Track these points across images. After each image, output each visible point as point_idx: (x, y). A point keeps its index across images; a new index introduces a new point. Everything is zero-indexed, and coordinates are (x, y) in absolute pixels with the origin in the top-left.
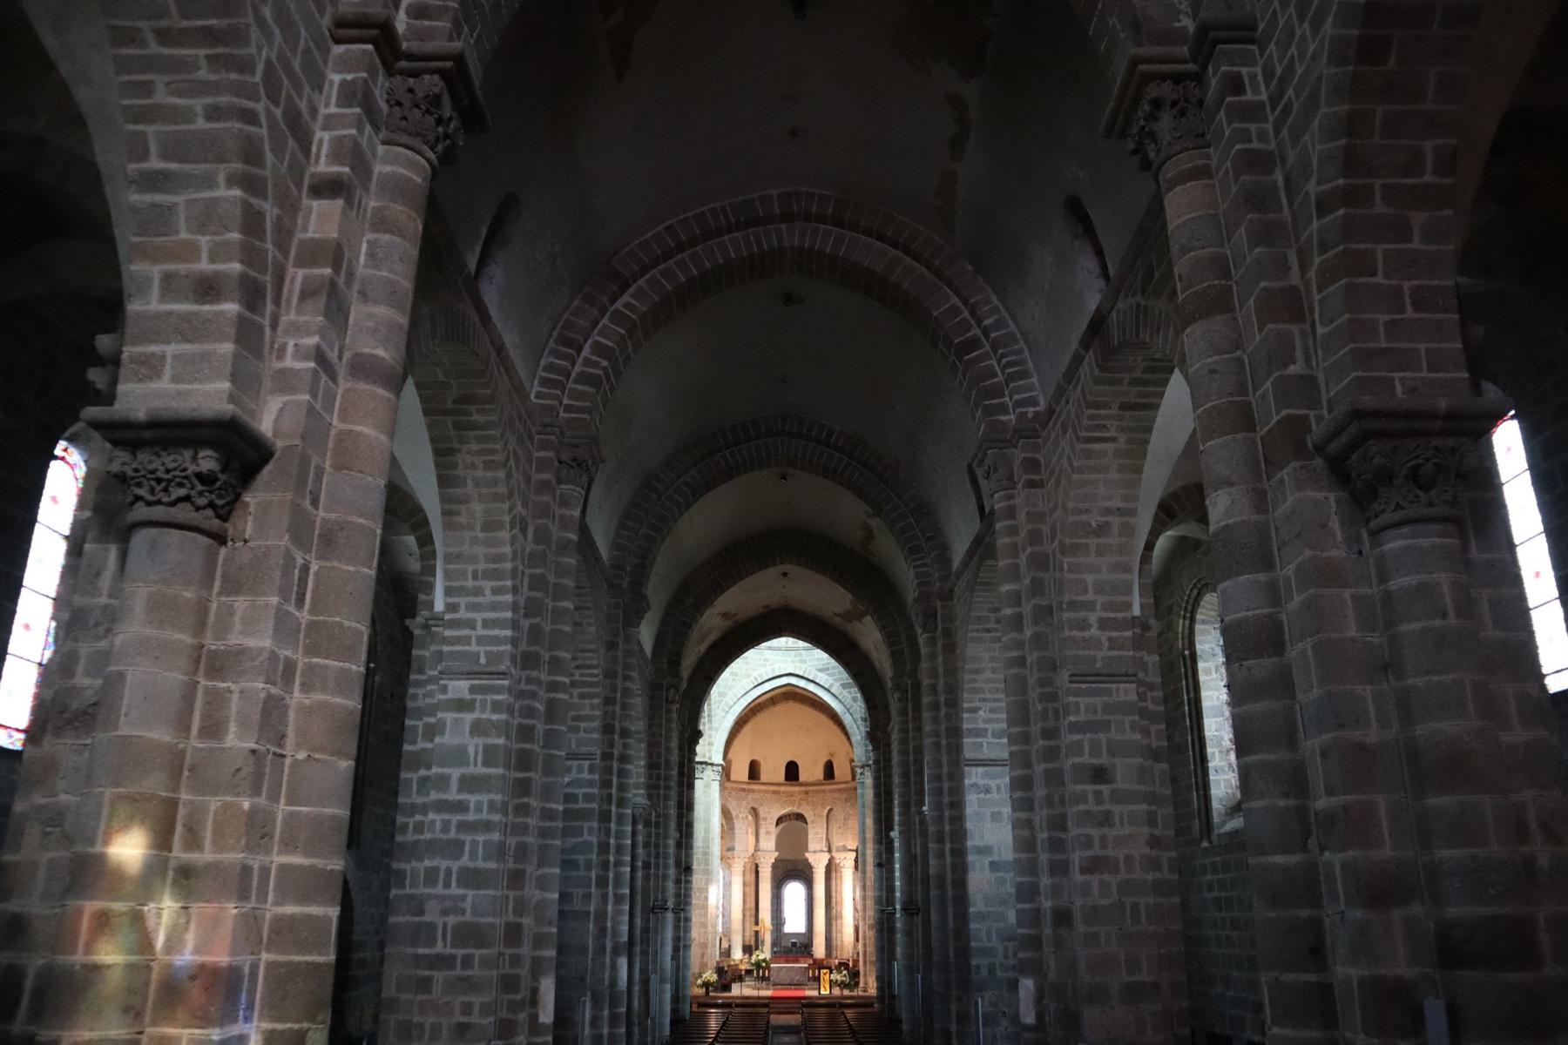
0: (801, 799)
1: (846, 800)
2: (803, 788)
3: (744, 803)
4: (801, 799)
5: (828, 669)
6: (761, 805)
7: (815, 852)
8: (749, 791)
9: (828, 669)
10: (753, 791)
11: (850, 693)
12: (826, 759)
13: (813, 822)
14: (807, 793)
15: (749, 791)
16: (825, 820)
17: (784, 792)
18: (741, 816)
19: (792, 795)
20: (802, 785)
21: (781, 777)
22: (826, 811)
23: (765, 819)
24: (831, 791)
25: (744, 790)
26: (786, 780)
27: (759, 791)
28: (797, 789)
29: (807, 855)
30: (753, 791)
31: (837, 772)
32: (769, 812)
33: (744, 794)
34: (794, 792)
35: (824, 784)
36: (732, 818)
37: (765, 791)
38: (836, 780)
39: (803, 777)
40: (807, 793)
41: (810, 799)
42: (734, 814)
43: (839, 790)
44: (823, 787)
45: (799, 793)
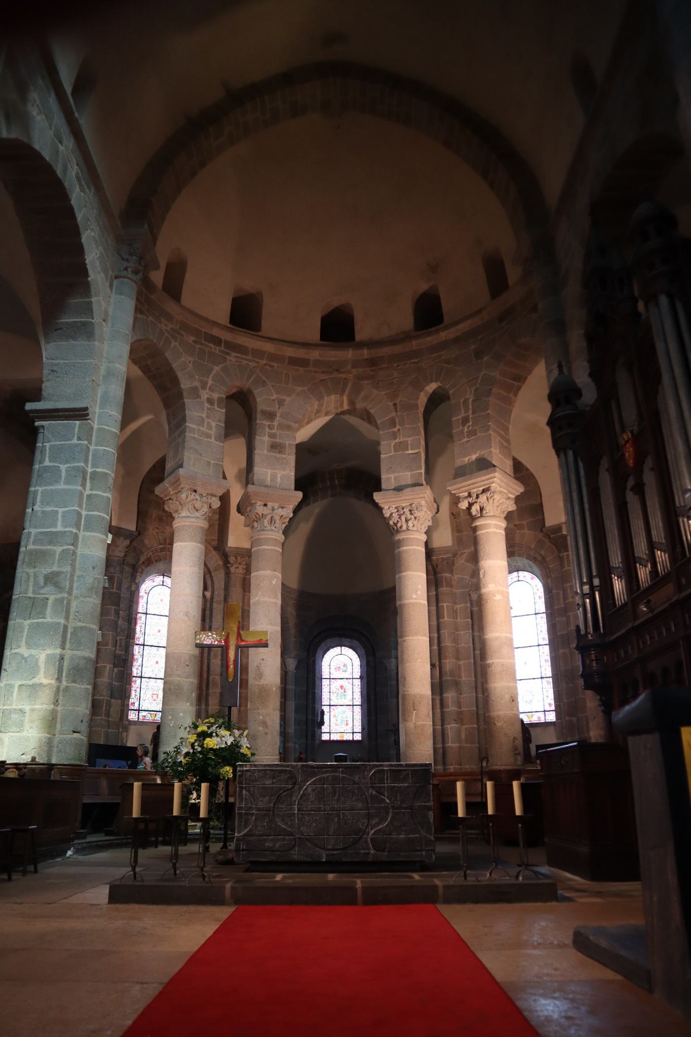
1: (478, 354)
2: (365, 353)
3: (216, 369)
6: (264, 384)
7: (399, 489)
8: (232, 347)
10: (241, 349)
12: (424, 286)
13: (393, 423)
15: (232, 347)
16: (421, 425)
17: (317, 363)
18: (205, 395)
21: (314, 333)
22: (423, 400)
23: (271, 416)
24: (444, 345)
25: (217, 341)
26: (322, 339)
27: (258, 354)
28: (349, 354)
29: (377, 497)
30: (241, 349)
31: (447, 305)
32: (281, 403)
36: (180, 395)
37: (273, 357)
38: (446, 321)
39: (362, 332)
40: (372, 362)
42: (185, 384)
43: (456, 340)
44: (414, 344)
45: (356, 364)
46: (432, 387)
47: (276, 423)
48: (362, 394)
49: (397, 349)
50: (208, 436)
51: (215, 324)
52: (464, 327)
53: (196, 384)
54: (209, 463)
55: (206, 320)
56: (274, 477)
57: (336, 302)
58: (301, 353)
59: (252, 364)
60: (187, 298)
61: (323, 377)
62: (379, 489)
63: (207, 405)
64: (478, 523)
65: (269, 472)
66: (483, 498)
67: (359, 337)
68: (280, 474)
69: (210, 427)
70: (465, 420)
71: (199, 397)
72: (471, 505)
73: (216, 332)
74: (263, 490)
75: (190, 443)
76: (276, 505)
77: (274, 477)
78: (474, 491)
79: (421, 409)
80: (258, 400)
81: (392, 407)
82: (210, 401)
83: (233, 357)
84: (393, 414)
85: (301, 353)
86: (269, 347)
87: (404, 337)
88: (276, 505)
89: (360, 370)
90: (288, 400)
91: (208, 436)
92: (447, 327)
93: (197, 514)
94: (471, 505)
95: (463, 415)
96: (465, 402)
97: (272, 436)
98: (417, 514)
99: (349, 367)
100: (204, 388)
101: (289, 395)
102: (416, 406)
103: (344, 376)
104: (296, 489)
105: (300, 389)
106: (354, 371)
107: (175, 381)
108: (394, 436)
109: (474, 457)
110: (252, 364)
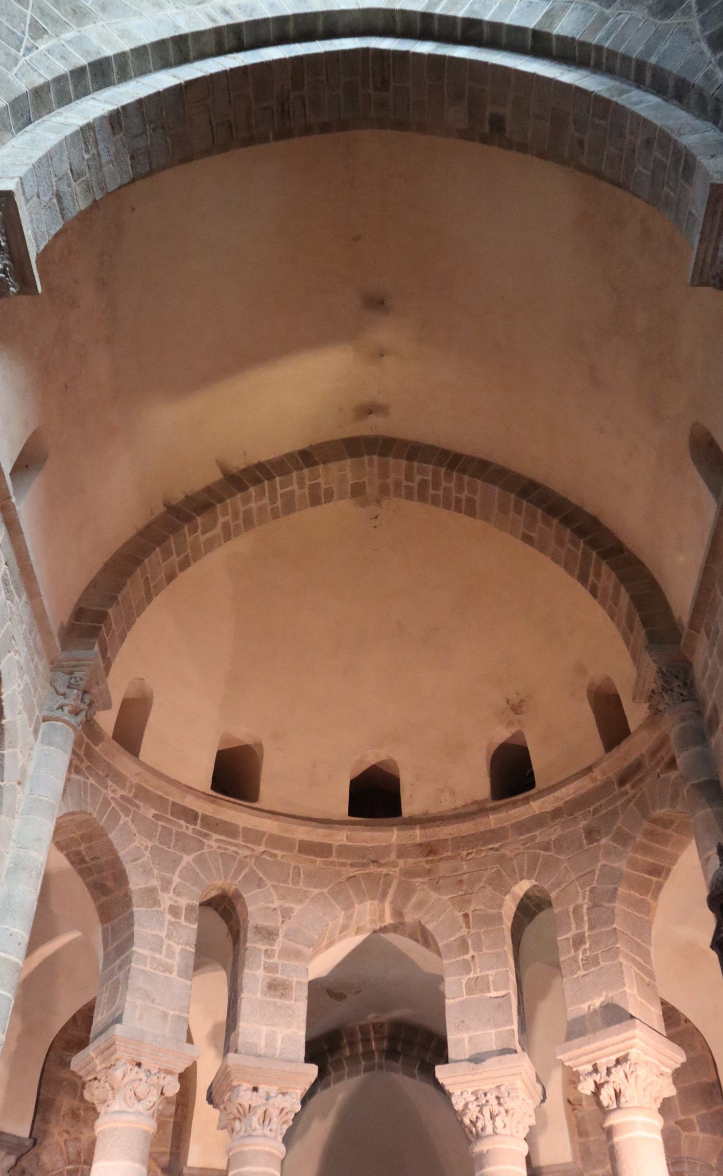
0: (410, 873)
1: (591, 834)
2: (418, 835)
3: (187, 859)
4: (410, 873)
6: (260, 884)
7: (477, 1059)
8: (212, 825)
10: (228, 830)
12: (502, 734)
13: (463, 946)
14: (429, 849)
15: (212, 825)
16: (508, 947)
17: (343, 850)
18: (166, 900)
19: (375, 857)
20: (413, 822)
21: (340, 806)
22: (509, 908)
23: (270, 935)
24: (539, 821)
25: (191, 816)
26: (351, 813)
30: (228, 830)
32: (286, 914)
33: (188, 829)
34: (385, 850)
35: (494, 810)
36: (126, 902)
37: (275, 841)
40: (429, 849)
41: (443, 868)
42: (136, 883)
43: (557, 813)
44: (492, 821)
45: (403, 852)
46: (523, 887)
47: (277, 947)
48: (414, 900)
49: (466, 828)
50: (168, 969)
51: (189, 789)
52: (567, 793)
53: (154, 882)
54: (165, 1015)
55: (176, 783)
56: (271, 1038)
57: (372, 758)
58: (318, 835)
59: (243, 852)
60: (148, 750)
61: (353, 872)
62: (446, 1060)
63: (168, 917)
64: (613, 1120)
65: (264, 1029)
66: (618, 1074)
67: (409, 808)
68: (281, 1033)
69: (171, 954)
70: (579, 941)
71: (156, 903)
72: (598, 1086)
73: (190, 802)
74: (251, 1062)
75: (136, 981)
76: (273, 1090)
77: (271, 1038)
78: (603, 1063)
79: (508, 923)
80: (250, 909)
81: (461, 920)
82: (174, 911)
83: (213, 841)
84: (464, 931)
85: (318, 835)
86: (269, 825)
87: (478, 810)
88: (273, 1090)
89: (411, 861)
90: (297, 908)
91: (168, 969)
92: (542, 794)
93: (140, 1107)
94: (598, 1086)
95: (574, 931)
96: (577, 910)
97: (270, 968)
98: (509, 1103)
99: (393, 856)
100: (165, 889)
101: (301, 901)
102: (499, 918)
103: (385, 870)
104: (309, 1059)
105: (315, 891)
106: (401, 862)
107: (121, 877)
108: (466, 967)
109: (597, 1002)
110: (243, 852)
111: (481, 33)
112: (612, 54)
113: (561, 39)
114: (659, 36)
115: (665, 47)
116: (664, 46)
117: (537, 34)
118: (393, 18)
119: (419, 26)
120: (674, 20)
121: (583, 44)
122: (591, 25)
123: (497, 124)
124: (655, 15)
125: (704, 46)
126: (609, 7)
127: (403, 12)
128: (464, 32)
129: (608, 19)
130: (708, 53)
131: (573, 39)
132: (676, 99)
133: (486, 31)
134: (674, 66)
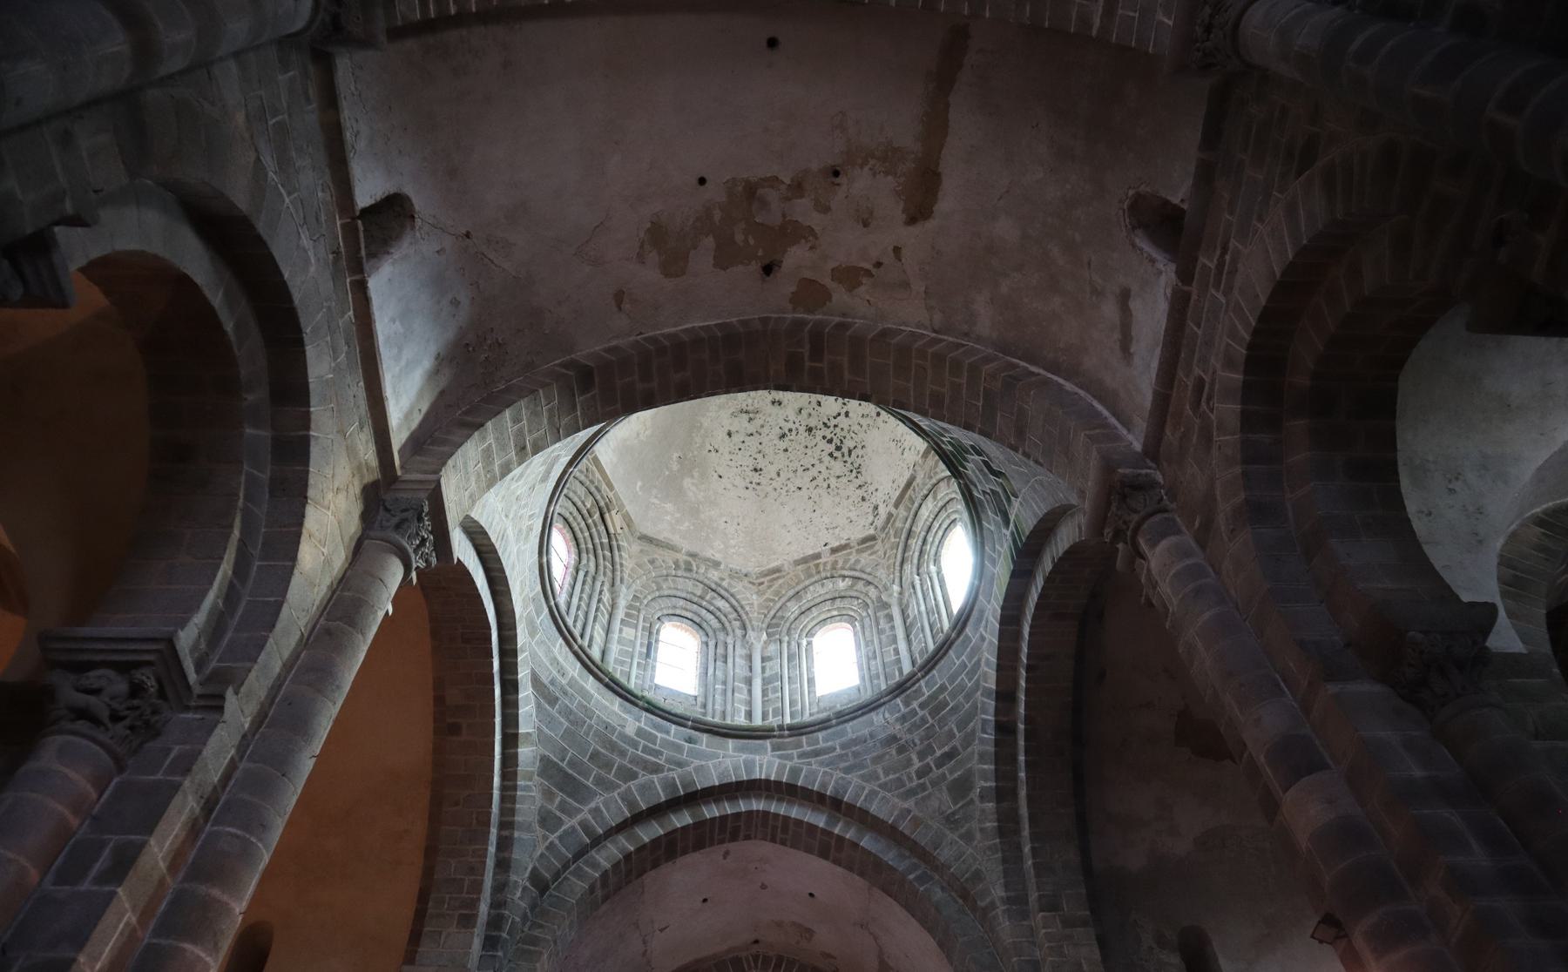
5: (553, 701)
9: (553, 701)
11: (548, 795)
111: (510, 694)
112: (513, 799)
113: (516, 755)
114: (529, 828)
115: (525, 837)
116: (525, 836)
117: (516, 736)
118: (510, 629)
119: (508, 647)
120: (539, 831)
121: (515, 773)
122: (527, 771)
123: (455, 729)
124: (539, 811)
125: (530, 869)
126: (538, 775)
127: (516, 635)
128: (509, 680)
129: (530, 780)
130: (527, 875)
131: (517, 766)
132: (497, 861)
133: (511, 697)
134: (517, 854)
